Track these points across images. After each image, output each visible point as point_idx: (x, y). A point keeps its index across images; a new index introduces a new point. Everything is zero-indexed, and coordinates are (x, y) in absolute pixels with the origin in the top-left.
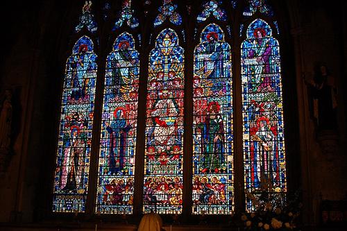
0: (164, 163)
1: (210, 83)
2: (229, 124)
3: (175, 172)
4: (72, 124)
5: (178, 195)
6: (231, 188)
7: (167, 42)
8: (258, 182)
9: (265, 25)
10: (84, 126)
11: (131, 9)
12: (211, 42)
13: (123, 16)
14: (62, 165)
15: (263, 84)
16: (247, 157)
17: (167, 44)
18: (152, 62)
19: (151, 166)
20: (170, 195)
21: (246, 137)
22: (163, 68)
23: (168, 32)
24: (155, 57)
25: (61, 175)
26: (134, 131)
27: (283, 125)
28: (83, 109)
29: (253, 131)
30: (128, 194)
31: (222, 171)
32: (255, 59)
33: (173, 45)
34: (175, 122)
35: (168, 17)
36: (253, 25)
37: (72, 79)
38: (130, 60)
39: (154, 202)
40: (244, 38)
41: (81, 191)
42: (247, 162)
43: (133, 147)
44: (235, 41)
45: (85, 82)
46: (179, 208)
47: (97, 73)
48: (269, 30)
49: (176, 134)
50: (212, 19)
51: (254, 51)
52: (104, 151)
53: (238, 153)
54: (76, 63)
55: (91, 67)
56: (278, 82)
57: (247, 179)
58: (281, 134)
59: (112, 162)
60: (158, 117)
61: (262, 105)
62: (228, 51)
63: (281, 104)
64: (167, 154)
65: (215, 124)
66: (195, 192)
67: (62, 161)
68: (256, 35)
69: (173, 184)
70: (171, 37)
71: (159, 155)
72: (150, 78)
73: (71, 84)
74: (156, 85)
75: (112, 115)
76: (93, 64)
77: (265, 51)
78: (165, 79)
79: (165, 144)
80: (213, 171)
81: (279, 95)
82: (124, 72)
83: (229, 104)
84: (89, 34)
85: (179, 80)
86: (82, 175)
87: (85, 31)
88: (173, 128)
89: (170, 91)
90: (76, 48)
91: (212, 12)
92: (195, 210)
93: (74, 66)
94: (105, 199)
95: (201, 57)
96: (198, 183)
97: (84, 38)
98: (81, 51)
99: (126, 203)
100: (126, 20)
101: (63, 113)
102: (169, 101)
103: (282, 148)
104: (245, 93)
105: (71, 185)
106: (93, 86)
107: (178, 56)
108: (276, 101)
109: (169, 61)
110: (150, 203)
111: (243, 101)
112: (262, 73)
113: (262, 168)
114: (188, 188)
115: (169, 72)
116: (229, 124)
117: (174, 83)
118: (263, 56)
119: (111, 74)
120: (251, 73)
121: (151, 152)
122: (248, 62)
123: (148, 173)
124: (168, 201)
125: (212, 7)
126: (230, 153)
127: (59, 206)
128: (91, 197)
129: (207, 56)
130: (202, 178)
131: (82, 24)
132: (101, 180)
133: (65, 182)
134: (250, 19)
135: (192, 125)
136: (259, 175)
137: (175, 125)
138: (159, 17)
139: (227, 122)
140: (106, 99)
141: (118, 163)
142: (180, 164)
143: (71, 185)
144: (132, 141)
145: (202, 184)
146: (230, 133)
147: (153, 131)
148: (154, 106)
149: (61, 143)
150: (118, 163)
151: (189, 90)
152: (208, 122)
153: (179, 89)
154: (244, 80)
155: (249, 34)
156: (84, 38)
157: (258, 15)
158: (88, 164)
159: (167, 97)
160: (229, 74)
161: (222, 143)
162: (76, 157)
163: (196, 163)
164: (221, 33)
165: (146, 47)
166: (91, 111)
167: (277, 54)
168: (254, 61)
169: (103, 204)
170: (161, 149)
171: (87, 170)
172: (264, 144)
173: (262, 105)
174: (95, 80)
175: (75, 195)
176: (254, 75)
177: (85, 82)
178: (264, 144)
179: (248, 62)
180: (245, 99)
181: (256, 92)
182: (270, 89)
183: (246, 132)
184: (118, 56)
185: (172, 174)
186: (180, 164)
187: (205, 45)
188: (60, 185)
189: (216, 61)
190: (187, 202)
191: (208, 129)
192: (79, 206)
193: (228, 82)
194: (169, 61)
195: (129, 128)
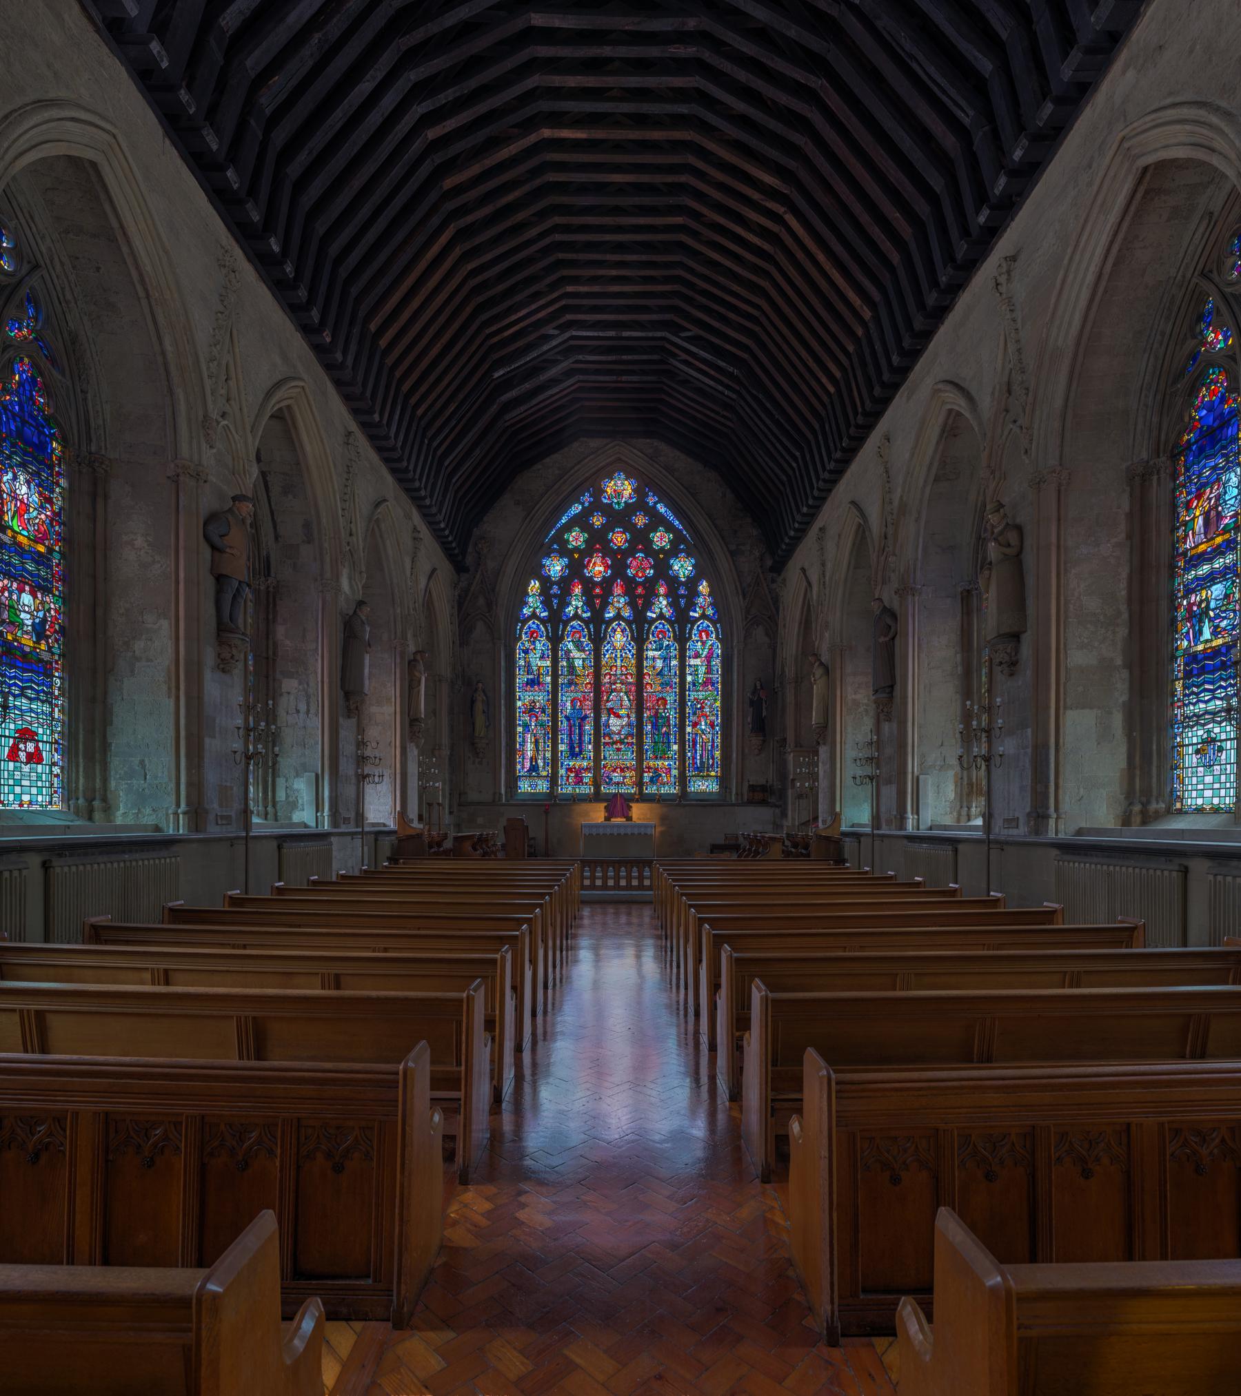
0: (619, 750)
1: (659, 680)
2: (675, 718)
3: (629, 758)
4: (530, 710)
5: (631, 777)
6: (675, 772)
7: (618, 636)
8: (698, 767)
9: (709, 626)
10: (542, 713)
11: (583, 595)
12: (660, 639)
13: (574, 603)
14: (523, 750)
15: (705, 684)
16: (689, 747)
17: (619, 639)
18: (605, 655)
19: (609, 753)
20: (625, 777)
21: (689, 729)
22: (616, 661)
23: (619, 625)
24: (607, 651)
25: (523, 759)
26: (591, 720)
27: (719, 721)
28: (541, 698)
29: (695, 725)
30: (587, 777)
31: (668, 757)
32: (699, 660)
33: (625, 639)
34: (628, 714)
35: (619, 609)
36: (699, 626)
37: (525, 666)
38: (583, 651)
39: (610, 782)
40: (690, 637)
41: (545, 773)
42: (689, 751)
43: (590, 735)
44: (682, 639)
45: (539, 670)
46: (633, 788)
47: (552, 662)
48: (712, 633)
49: (629, 725)
50: (661, 616)
51: (698, 652)
52: (563, 737)
53: (682, 743)
54: (528, 649)
55: (544, 654)
56: (718, 682)
57: (689, 764)
58: (717, 728)
59: (571, 748)
60: (613, 708)
61: (703, 702)
62: (675, 650)
63: (719, 702)
64: (621, 742)
65: (663, 717)
66: (646, 775)
67: (524, 746)
68: (701, 636)
69: (627, 768)
70: (622, 631)
71: (615, 743)
72: (604, 671)
73: (524, 671)
74: (610, 678)
75: (569, 704)
76: (546, 652)
77: (708, 653)
78: (619, 672)
79: (619, 733)
80: (661, 757)
81: (718, 695)
82: (578, 663)
83: (675, 700)
84: (538, 618)
85: (631, 675)
86: (544, 758)
87: (534, 615)
88: (626, 719)
89: (622, 684)
90: (526, 633)
91: (661, 609)
92: (646, 789)
93: (526, 652)
94: (567, 780)
95: (650, 654)
96: (649, 768)
97: (534, 623)
98: (531, 636)
99: (586, 784)
100: (577, 608)
101: (520, 699)
102: (622, 694)
103: (718, 741)
104: (689, 690)
105: (534, 768)
106: (547, 674)
107: (630, 651)
108: (715, 700)
109: (621, 656)
110: (608, 784)
111: (687, 698)
112: (705, 673)
113: (701, 756)
114: (640, 770)
115: (622, 666)
116: (675, 718)
117: (627, 678)
118: (706, 657)
119: (565, 664)
120: (695, 673)
121: (607, 740)
122: (693, 662)
123: (605, 758)
124: (623, 782)
125: (661, 603)
126: (675, 743)
127: (525, 787)
128: (553, 779)
129: (657, 653)
130: (651, 763)
131: (530, 607)
132: (562, 763)
133: (527, 765)
134: (697, 619)
135: (644, 717)
136: (698, 762)
137: (628, 716)
138: (610, 608)
139: (673, 715)
140: (562, 688)
141: (577, 749)
142: (633, 751)
143: (534, 768)
144: (588, 727)
145: (651, 768)
146: (675, 726)
147: (609, 720)
148: (608, 698)
149: (520, 729)
150: (577, 749)
151: (640, 685)
152: (656, 715)
153: (630, 683)
154: (689, 678)
155: (695, 635)
156: (534, 623)
157: (704, 616)
158: (550, 749)
159: (621, 691)
160: (676, 674)
161: (669, 734)
162: (536, 742)
163: (647, 750)
164: (669, 631)
165: (598, 640)
166: (548, 700)
167: (718, 655)
168: (698, 662)
169: (566, 784)
170: (616, 737)
171: (548, 755)
172: (704, 736)
173: (703, 702)
174: (550, 669)
175: (539, 776)
176: (697, 675)
177: (539, 670)
178: (704, 736)
179: (693, 662)
180: (689, 696)
181: (697, 691)
182: (710, 688)
183: (689, 726)
184: (571, 646)
185: (626, 759)
186: (633, 751)
187: (655, 642)
188: (523, 768)
189: (665, 659)
190: (640, 783)
191: (657, 721)
192: (543, 786)
193: (674, 680)
194: (621, 656)
195: (586, 717)
